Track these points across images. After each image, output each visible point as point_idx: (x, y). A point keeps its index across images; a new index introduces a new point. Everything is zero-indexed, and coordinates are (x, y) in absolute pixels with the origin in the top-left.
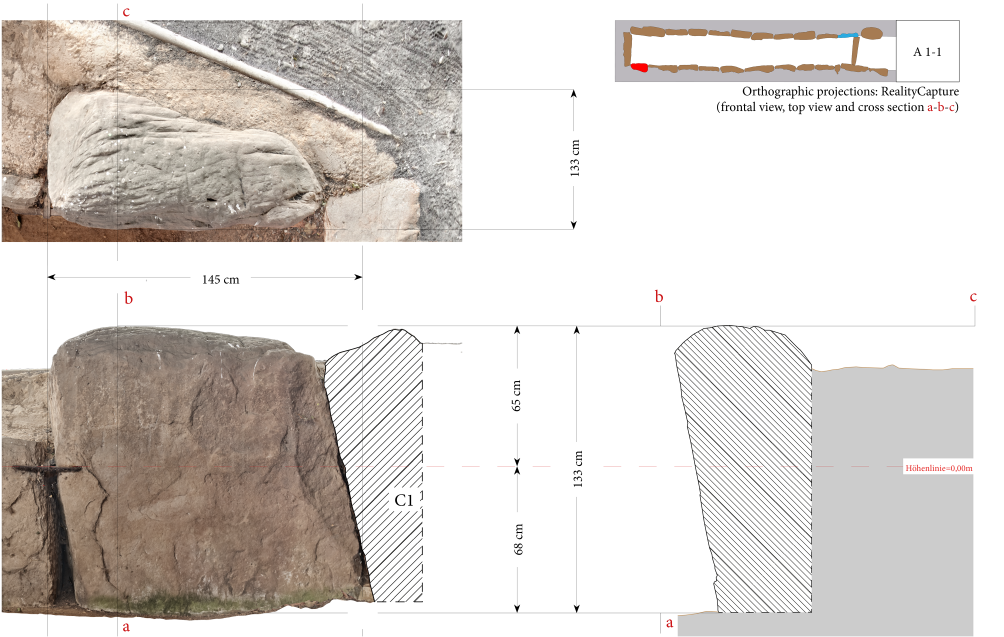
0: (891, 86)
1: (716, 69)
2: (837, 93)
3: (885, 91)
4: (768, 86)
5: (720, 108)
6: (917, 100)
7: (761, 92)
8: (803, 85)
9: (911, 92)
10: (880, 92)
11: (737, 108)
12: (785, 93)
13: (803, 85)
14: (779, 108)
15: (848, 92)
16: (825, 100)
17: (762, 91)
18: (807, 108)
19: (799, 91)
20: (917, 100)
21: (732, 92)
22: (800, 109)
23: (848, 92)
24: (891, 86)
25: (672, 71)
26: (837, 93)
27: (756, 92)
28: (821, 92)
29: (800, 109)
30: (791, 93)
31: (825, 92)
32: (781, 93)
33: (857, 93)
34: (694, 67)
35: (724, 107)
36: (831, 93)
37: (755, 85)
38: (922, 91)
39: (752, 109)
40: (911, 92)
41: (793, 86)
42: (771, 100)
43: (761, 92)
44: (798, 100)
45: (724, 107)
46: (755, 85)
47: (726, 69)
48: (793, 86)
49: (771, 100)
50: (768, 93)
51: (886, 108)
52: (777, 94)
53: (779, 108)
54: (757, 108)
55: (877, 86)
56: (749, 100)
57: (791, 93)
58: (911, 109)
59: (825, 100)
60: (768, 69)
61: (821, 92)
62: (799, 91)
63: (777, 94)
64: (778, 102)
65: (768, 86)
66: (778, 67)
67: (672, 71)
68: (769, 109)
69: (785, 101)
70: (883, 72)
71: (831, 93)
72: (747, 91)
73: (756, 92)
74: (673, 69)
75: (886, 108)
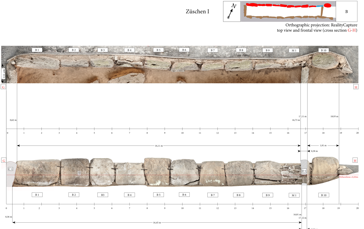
0: (334, 23)
2: (318, 25)
4: (294, 23)
7: (292, 25)
8: (306, 23)
9: (341, 25)
12: (300, 25)
13: (306, 23)
15: (321, 25)
17: (293, 25)
19: (305, 25)
21: (282, 25)
23: (321, 25)
24: (334, 23)
26: (318, 25)
27: (290, 25)
28: (312, 25)
31: (314, 25)
32: (299, 26)
33: (324, 26)
36: (316, 25)
40: (341, 25)
41: (303, 23)
42: (295, 28)
43: (292, 25)
48: (303, 23)
49: (295, 28)
50: (294, 26)
51: (334, 31)
52: (297, 26)
55: (330, 23)
57: (302, 26)
58: (342, 31)
61: (312, 25)
62: (305, 25)
64: (297, 29)
65: (294, 23)
71: (316, 25)
72: (287, 25)
73: (290, 25)
75: (334, 31)
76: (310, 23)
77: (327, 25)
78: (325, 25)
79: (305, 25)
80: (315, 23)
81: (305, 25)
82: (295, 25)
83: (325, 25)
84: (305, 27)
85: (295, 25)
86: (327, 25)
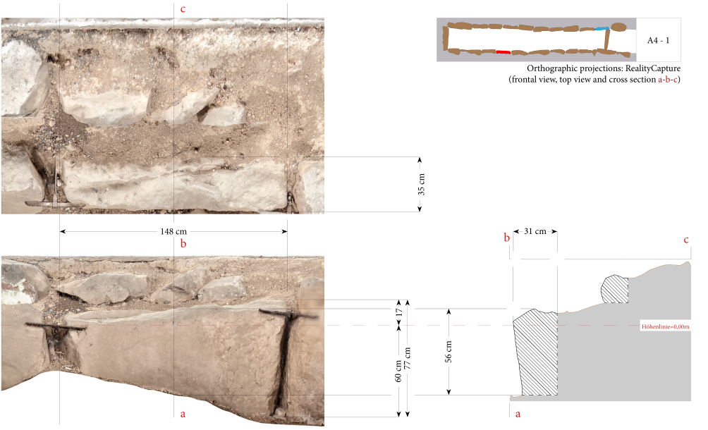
0: (632, 64)
1: (509, 52)
3: (628, 68)
4: (546, 64)
5: (511, 80)
6: (651, 75)
9: (646, 69)
10: (625, 69)
11: (527, 80)
12: (557, 69)
14: (553, 80)
15: (602, 69)
16: (586, 74)
17: (542, 68)
18: (573, 80)
19: (567, 68)
20: (651, 75)
21: (519, 68)
22: (568, 81)
23: (602, 69)
24: (632, 64)
25: (477, 54)
27: (537, 69)
29: (568, 81)
30: (562, 70)
31: (586, 69)
33: (608, 69)
35: (514, 79)
37: (536, 64)
38: (655, 68)
39: (534, 81)
40: (646, 69)
41: (563, 64)
42: (547, 75)
44: (567, 74)
45: (514, 79)
46: (536, 64)
48: (563, 64)
49: (547, 75)
50: (545, 69)
51: (629, 80)
52: (552, 70)
53: (553, 80)
54: (538, 80)
55: (623, 64)
56: (531, 75)
57: (562, 70)
58: (646, 80)
59: (586, 74)
60: (545, 52)
62: (567, 68)
63: (552, 70)
64: (552, 76)
65: (546, 64)
66: (552, 51)
67: (477, 54)
68: (546, 81)
69: (557, 75)
70: (627, 55)
72: (530, 68)
73: (537, 69)
74: (478, 52)
75: (629, 80)
76: (578, 64)
77: (619, 69)
78: (610, 69)
79: (569, 69)
80: (590, 64)
81: (569, 69)
82: (548, 69)
83: (610, 69)
85: (548, 69)
86: (619, 69)
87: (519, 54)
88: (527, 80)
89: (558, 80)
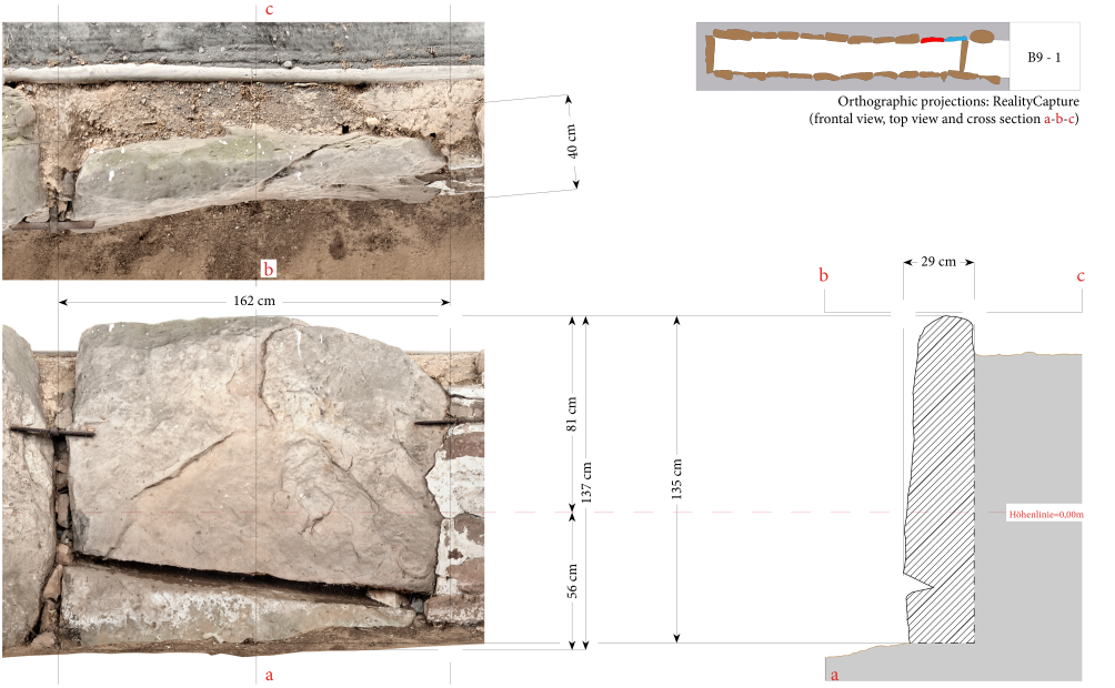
0: (1004, 95)
2: (944, 103)
3: (997, 101)
4: (868, 95)
6: (1033, 111)
8: (906, 94)
9: (1026, 102)
10: (991, 102)
11: (838, 120)
12: (885, 103)
13: (906, 94)
14: (879, 120)
15: (956, 102)
16: (930, 111)
17: (860, 101)
18: (910, 120)
19: (901, 101)
20: (1033, 111)
21: (826, 101)
22: (902, 121)
23: (956, 102)
24: (1004, 95)
25: (760, 79)
26: (944, 103)
27: (853, 103)
28: (925, 102)
29: (902, 121)
30: (892, 103)
33: (965, 103)
34: (784, 74)
35: (818, 119)
37: (852, 95)
38: (1038, 101)
39: (849, 120)
40: (1026, 102)
42: (870, 111)
44: (901, 111)
45: (818, 119)
46: (852, 95)
47: (820, 77)
49: (870, 111)
50: (867, 103)
51: (998, 120)
52: (877, 104)
53: (879, 120)
54: (855, 120)
55: (988, 95)
56: (845, 111)
57: (892, 103)
58: (1026, 121)
59: (930, 111)
61: (925, 102)
62: (901, 101)
63: (877, 104)
64: (878, 113)
65: (868, 95)
66: (878, 74)
67: (760, 79)
68: (868, 121)
69: (885, 112)
70: (995, 80)
72: (843, 101)
73: (853, 103)
74: (761, 76)
75: (998, 120)
77: (982, 103)
78: (969, 103)
82: (870, 103)
83: (969, 103)
84: (904, 107)
85: (870, 103)
86: (982, 103)
87: (824, 80)
88: (838, 120)
89: (887, 119)
